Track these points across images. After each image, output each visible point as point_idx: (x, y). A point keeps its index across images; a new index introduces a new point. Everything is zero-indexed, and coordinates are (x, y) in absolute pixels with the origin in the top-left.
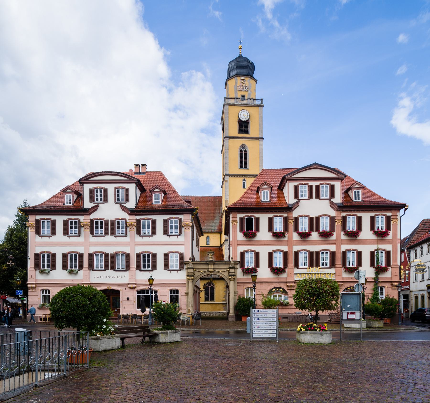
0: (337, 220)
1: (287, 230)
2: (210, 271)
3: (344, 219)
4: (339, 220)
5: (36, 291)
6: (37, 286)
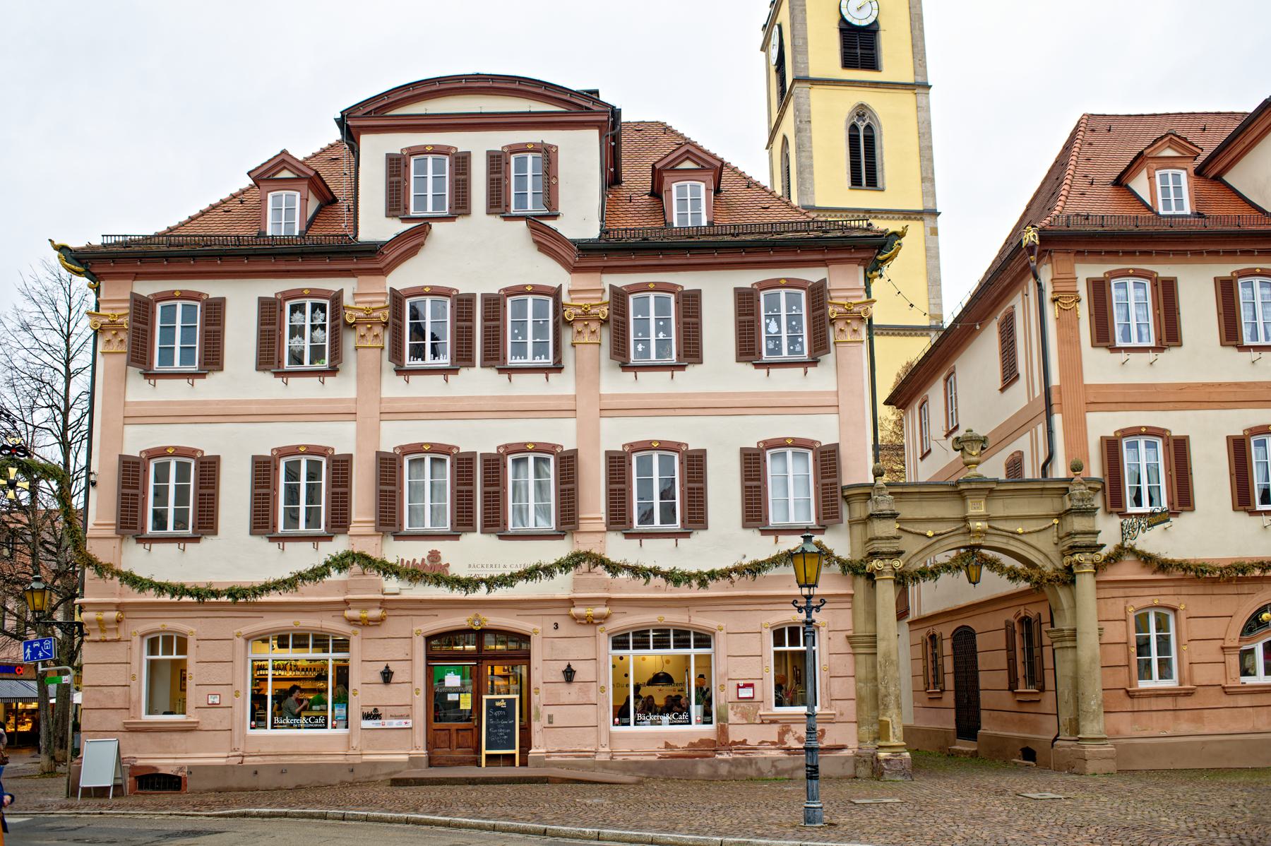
2: (970, 531)
5: (118, 641)
6: (128, 615)
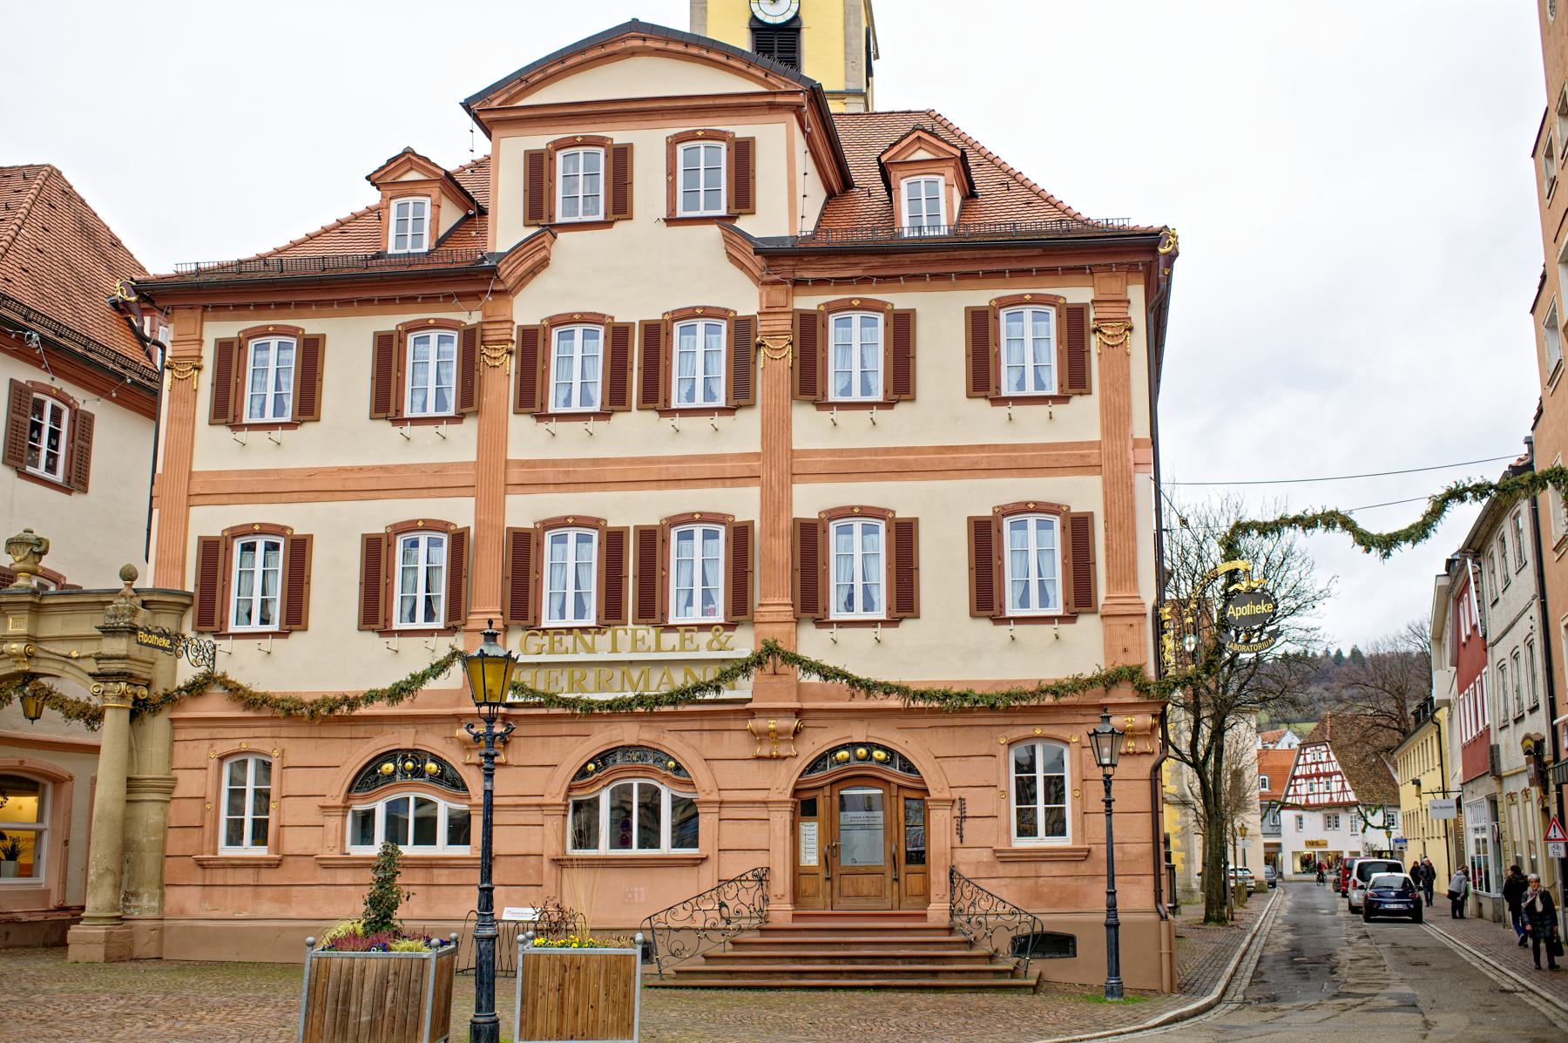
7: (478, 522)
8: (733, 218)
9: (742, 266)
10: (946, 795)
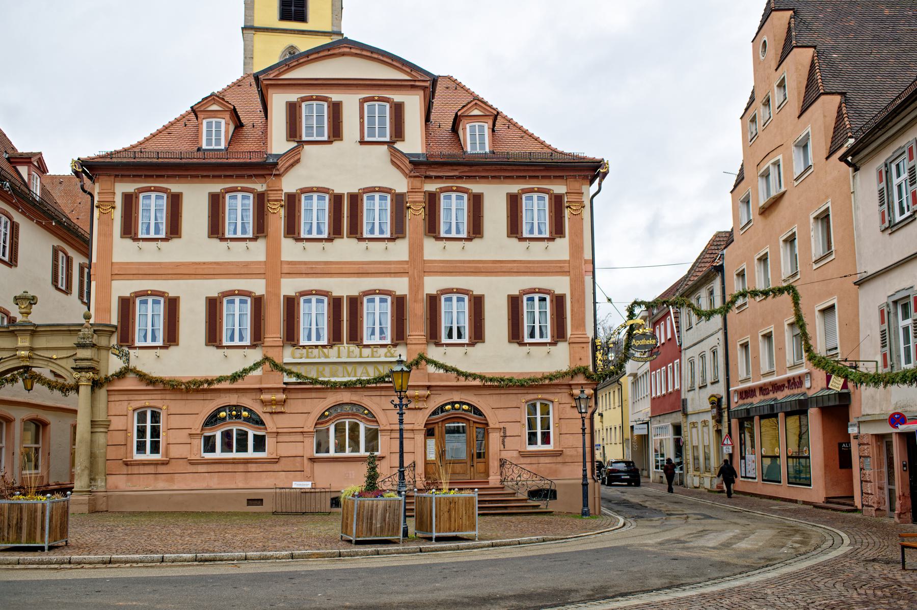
0: (411, 202)
1: (263, 232)
3: (432, 201)
4: (415, 202)
7: (267, 291)
8: (394, 143)
9: (398, 167)
10: (497, 426)
